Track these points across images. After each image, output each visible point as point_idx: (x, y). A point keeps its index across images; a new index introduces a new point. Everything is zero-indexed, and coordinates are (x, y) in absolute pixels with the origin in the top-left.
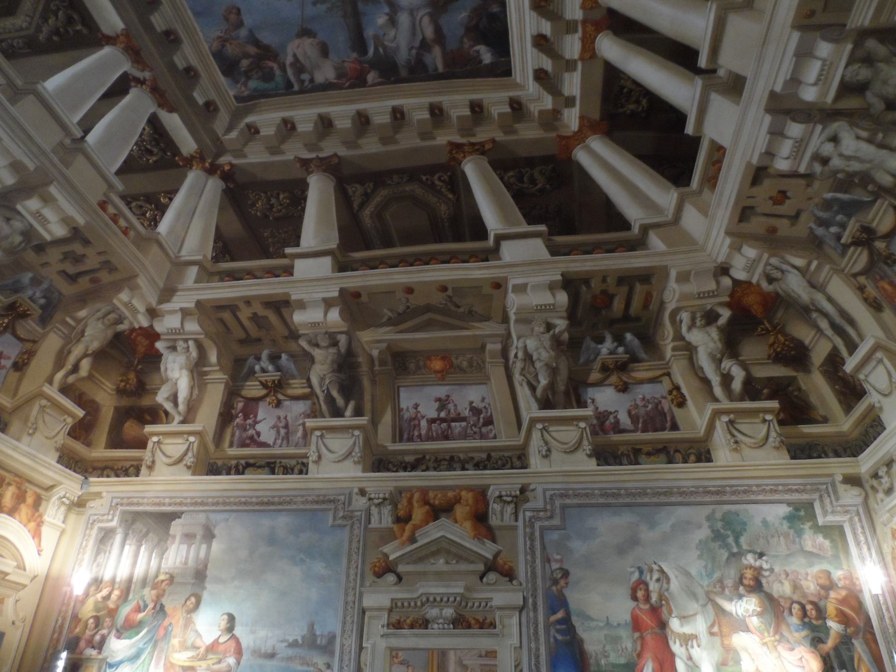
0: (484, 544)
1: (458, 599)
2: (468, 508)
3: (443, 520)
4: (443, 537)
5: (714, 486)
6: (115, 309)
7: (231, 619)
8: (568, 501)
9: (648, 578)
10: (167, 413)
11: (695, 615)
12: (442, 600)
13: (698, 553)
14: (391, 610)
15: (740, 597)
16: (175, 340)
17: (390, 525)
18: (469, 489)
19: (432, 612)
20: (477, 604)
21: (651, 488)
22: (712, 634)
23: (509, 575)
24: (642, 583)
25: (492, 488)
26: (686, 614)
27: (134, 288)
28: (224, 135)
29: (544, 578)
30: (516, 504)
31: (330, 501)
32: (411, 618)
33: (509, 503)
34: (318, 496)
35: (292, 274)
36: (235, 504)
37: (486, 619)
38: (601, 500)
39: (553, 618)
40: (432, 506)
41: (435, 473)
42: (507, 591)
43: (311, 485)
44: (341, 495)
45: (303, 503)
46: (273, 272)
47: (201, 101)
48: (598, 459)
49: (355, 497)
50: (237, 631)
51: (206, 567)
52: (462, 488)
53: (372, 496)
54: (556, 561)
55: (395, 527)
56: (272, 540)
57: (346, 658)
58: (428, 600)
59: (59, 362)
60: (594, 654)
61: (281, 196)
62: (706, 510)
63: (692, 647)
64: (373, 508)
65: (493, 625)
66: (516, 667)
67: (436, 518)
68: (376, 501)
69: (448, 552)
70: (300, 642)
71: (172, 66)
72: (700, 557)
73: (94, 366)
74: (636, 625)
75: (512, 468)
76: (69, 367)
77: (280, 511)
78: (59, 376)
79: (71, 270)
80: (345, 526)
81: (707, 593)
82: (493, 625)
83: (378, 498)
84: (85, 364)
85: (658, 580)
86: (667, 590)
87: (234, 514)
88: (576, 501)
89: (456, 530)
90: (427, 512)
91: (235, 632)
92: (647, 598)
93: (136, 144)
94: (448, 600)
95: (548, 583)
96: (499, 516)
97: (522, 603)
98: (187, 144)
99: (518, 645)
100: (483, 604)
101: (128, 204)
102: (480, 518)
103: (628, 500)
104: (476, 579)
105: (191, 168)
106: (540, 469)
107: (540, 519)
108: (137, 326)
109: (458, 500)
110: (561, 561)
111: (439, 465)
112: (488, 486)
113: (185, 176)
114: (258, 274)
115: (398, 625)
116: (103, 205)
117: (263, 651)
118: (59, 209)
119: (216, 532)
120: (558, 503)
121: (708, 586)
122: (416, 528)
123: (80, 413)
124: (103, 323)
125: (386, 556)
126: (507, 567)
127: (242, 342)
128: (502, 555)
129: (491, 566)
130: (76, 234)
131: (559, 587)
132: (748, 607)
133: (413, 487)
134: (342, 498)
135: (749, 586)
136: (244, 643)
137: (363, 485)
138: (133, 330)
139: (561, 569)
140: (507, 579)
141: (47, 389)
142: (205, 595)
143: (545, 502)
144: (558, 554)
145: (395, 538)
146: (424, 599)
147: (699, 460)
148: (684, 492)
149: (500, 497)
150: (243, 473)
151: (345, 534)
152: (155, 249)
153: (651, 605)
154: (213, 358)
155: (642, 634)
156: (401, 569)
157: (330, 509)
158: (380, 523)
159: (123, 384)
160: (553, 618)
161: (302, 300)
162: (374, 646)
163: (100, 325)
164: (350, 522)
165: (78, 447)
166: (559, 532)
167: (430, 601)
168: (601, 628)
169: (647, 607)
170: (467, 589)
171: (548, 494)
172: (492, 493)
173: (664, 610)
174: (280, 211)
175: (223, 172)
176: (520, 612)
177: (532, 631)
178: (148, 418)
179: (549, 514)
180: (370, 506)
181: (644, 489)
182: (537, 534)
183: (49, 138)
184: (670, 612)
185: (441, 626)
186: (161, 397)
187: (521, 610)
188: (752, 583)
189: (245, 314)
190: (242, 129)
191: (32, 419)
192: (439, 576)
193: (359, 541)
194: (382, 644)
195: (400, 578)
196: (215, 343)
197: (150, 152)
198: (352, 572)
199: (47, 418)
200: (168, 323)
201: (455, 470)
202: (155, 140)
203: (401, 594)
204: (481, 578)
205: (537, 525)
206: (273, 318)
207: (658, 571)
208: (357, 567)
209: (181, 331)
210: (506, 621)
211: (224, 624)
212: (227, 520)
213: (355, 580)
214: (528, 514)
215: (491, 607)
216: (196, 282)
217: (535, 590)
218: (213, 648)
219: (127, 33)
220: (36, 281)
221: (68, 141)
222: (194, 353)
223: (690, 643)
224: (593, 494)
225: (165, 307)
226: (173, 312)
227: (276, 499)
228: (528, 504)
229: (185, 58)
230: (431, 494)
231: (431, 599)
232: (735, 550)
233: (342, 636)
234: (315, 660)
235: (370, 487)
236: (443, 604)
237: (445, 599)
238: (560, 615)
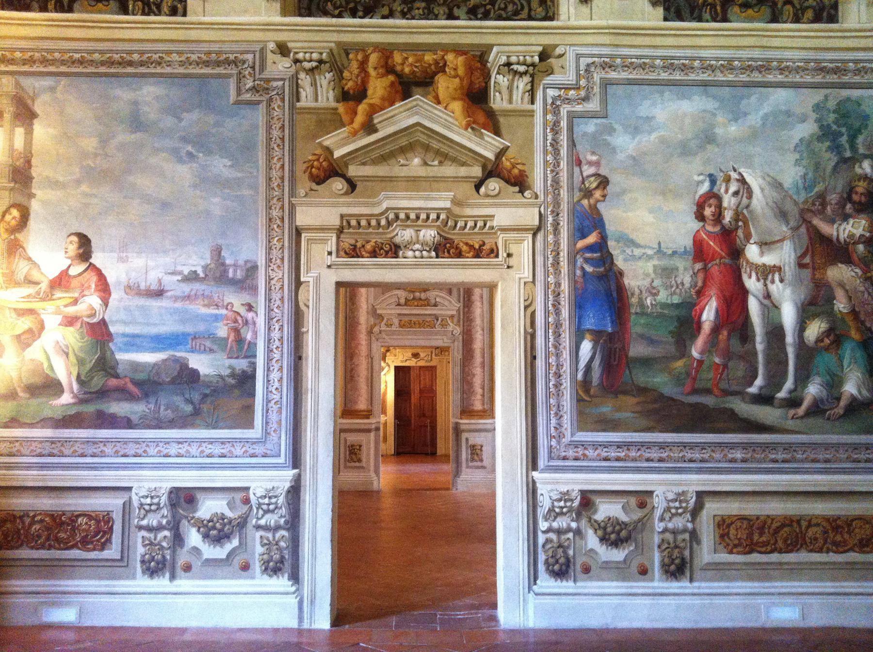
0: (481, 136)
1: (443, 216)
2: (457, 80)
3: (418, 98)
4: (418, 124)
5: (831, 61)
7: (84, 242)
8: (613, 75)
9: (723, 190)
11: (781, 241)
12: (418, 218)
13: (797, 156)
14: (340, 231)
15: (846, 218)
17: (333, 104)
18: (459, 50)
19: (404, 235)
20: (470, 224)
21: (740, 60)
22: (801, 266)
23: (520, 183)
24: (713, 196)
25: (495, 49)
26: (769, 239)
29: (571, 189)
30: (532, 76)
31: (228, 62)
32: (372, 243)
33: (521, 74)
34: (209, 53)
36: (63, 62)
37: (484, 244)
38: (664, 76)
39: (581, 244)
40: (399, 76)
41: (404, 22)
42: (516, 206)
43: (194, 35)
44: (247, 52)
45: (182, 64)
48: (667, 9)
49: (270, 57)
50: (97, 259)
51: (28, 162)
52: (447, 48)
53: (300, 56)
54: (590, 163)
55: (341, 108)
56: (136, 123)
57: (276, 296)
58: (397, 217)
60: (637, 292)
62: (818, 96)
63: (773, 282)
64: (302, 75)
65: (493, 252)
66: (526, 307)
67: (406, 95)
68: (307, 65)
69: (427, 148)
70: (202, 275)
72: (797, 163)
74: (699, 252)
75: (530, 18)
77: (143, 75)
80: (258, 103)
81: (802, 212)
82: (493, 252)
83: (311, 61)
85: (736, 193)
86: (747, 207)
87: (64, 81)
88: (624, 75)
89: (439, 115)
90: (392, 84)
91: (92, 260)
92: (718, 217)
94: (428, 217)
95: (577, 195)
96: (506, 96)
97: (537, 223)
99: (531, 279)
100: (480, 224)
102: (476, 97)
103: (704, 77)
104: (469, 188)
106: (573, 22)
107: (568, 101)
109: (441, 68)
110: (597, 164)
111: (410, 9)
112: (490, 47)
115: (354, 252)
117: (143, 286)
119: (38, 108)
120: (597, 76)
121: (806, 202)
122: (374, 109)
125: (329, 151)
126: (516, 171)
128: (510, 153)
129: (492, 170)
131: (592, 201)
132: (855, 231)
133: (368, 44)
134: (250, 57)
135: (860, 203)
136: (111, 279)
137: (282, 37)
139: (597, 175)
140: (517, 189)
142: (35, 206)
143: (578, 75)
144: (593, 153)
145: (343, 125)
146: (392, 216)
147: (817, 19)
148: (787, 67)
149: (508, 64)
150: (70, 10)
151: (259, 115)
153: (723, 227)
155: (706, 265)
156: (353, 171)
157: (229, 76)
158: (316, 100)
160: (581, 244)
162: (318, 279)
164: (265, 97)
166: (595, 120)
167: (397, 218)
168: (650, 258)
169: (717, 229)
170: (455, 202)
171: (584, 62)
172: (496, 58)
173: (740, 233)
176: (535, 235)
177: (551, 260)
179: (583, 93)
180: (297, 73)
181: (730, 60)
182: (564, 124)
184: (748, 237)
185: (417, 253)
187: (535, 232)
188: (863, 199)
192: (414, 183)
193: (282, 127)
194: (330, 278)
195: (352, 185)
198: (275, 174)
201: (436, 17)
203: (356, 208)
204: (478, 187)
205: (564, 110)
207: (738, 180)
208: (283, 166)
210: (513, 249)
211: (73, 248)
212: (52, 89)
213: (281, 186)
214: (551, 93)
215: (492, 228)
217: (557, 203)
218: (61, 281)
223: (770, 277)
224: (653, 66)
227: (136, 57)
228: (551, 77)
230: (397, 58)
231: (402, 216)
232: (848, 154)
233: (267, 266)
234: (227, 300)
235: (296, 41)
236: (420, 223)
237: (423, 216)
238: (592, 239)
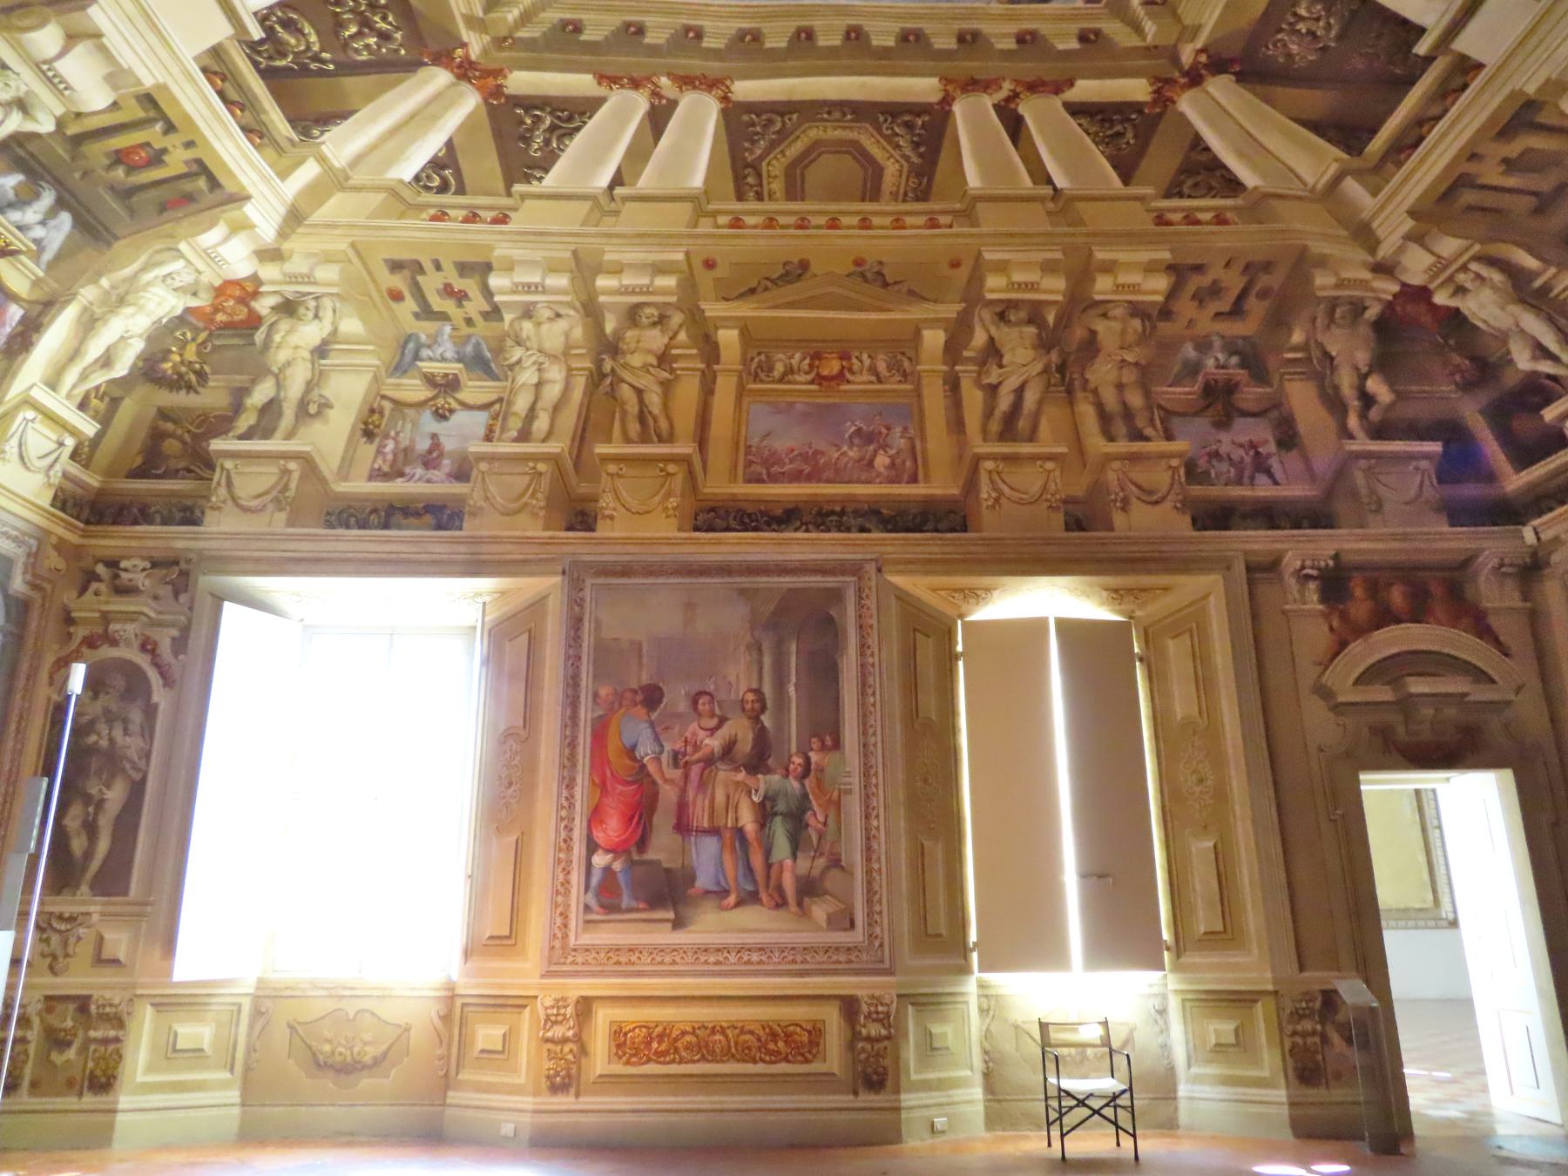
6: (1333, 304)
10: (1554, 378)
16: (1450, 279)
27: (1322, 262)
28: (1144, 39)
35: (1480, 66)
46: (1449, 91)
47: (1074, 44)
59: (1335, 404)
61: (1303, 12)
71: (1007, 55)
73: (1391, 383)
76: (1355, 404)
78: (1353, 422)
79: (1225, 305)
84: (1375, 385)
93: (1097, 144)
98: (1136, 89)
101: (1181, 195)
105: (1174, 102)
108: (1390, 298)
113: (1182, 115)
114: (1435, 110)
116: (1161, 220)
118: (1129, 266)
123: (1435, 447)
124: (1339, 326)
127: (1538, 211)
130: (1179, 272)
138: (1389, 306)
141: (1354, 446)
152: (1274, 203)
154: (1530, 262)
159: (1458, 377)
161: (1548, 81)
163: (1336, 331)
165: (1470, 490)
174: (1329, 27)
175: (1206, 66)
178: (1536, 399)
183: (1035, 219)
186: (1524, 361)
189: (1492, 174)
190: (1147, 14)
191: (1364, 491)
196: (1504, 241)
197: (1119, 135)
199: (1382, 478)
200: (1417, 266)
202: (1103, 120)
206: (1537, 142)
209: (1442, 264)
216: (1374, 194)
219: (946, 80)
220: (1203, 345)
221: (1051, 205)
222: (1497, 277)
225: (1384, 251)
226: (1401, 250)
229: (1005, 36)
